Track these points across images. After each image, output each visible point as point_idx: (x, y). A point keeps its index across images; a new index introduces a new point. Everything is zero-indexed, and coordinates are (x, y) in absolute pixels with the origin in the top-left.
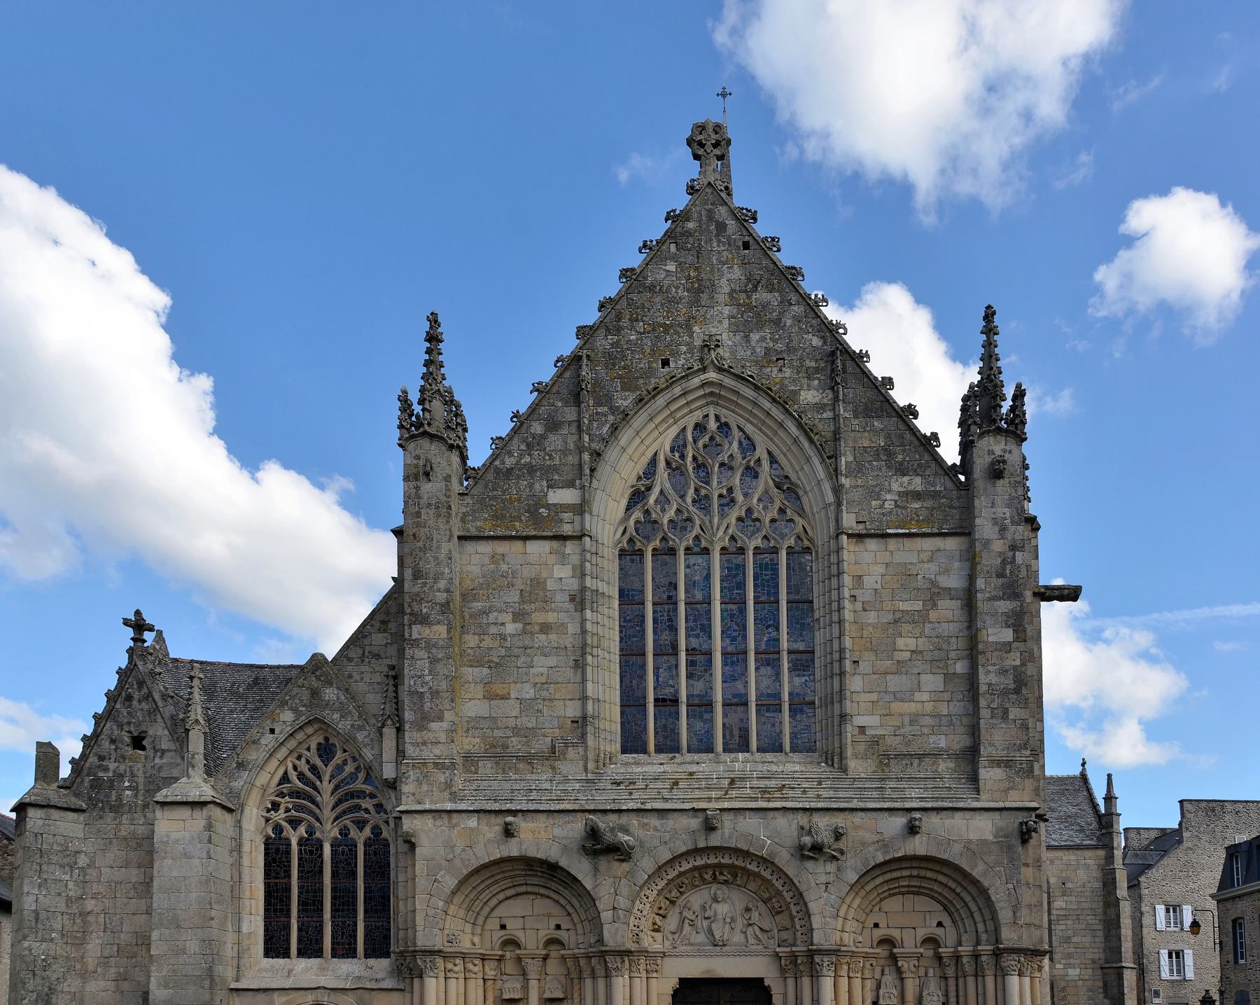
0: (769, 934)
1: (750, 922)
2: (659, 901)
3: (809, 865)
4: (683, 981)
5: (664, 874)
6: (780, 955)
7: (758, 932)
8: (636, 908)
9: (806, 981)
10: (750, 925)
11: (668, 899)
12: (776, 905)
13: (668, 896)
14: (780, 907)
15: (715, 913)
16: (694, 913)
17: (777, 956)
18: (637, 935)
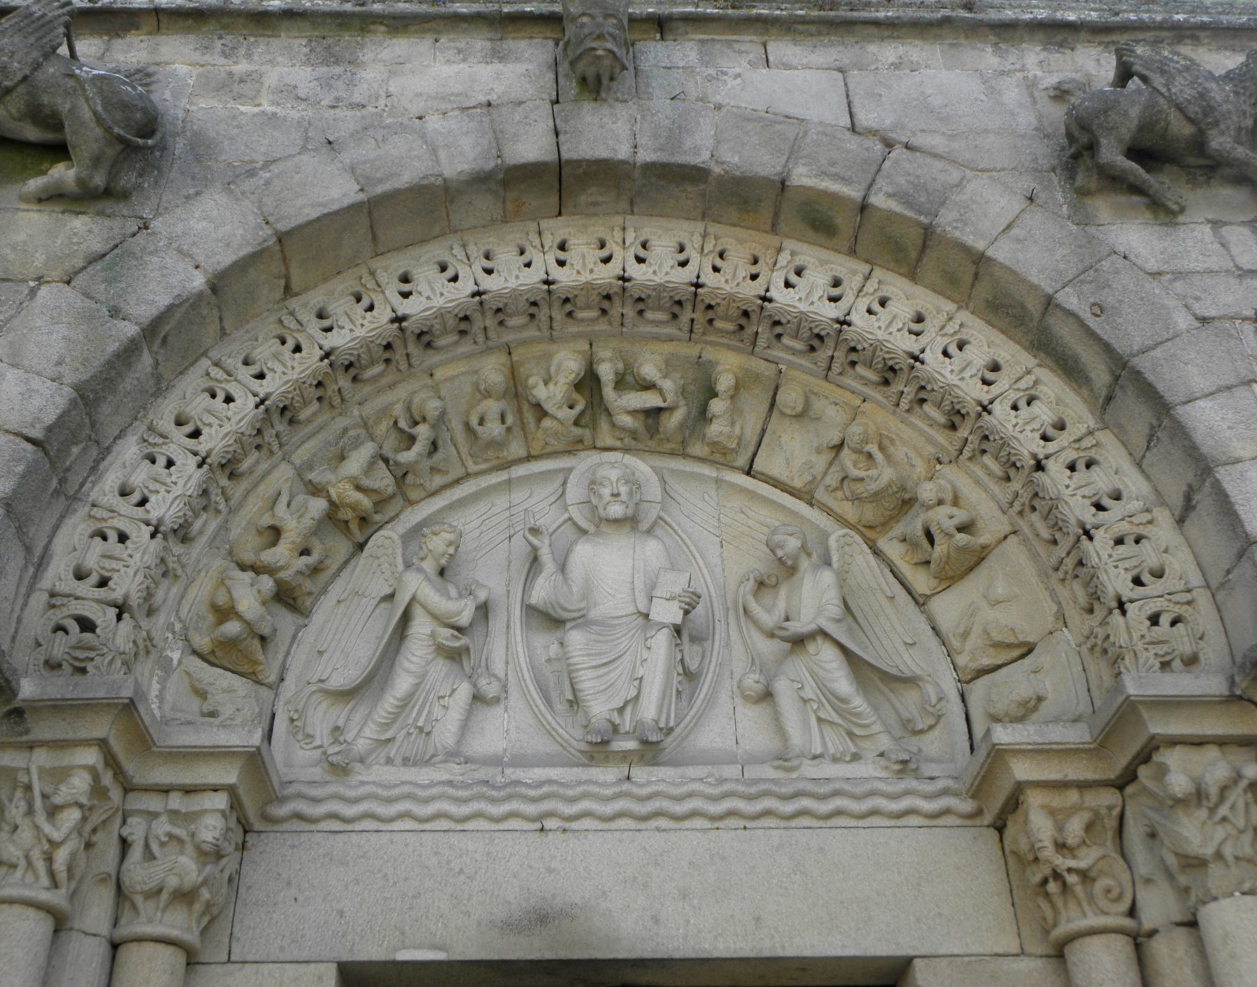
2: (266, 489)
5: (314, 326)
6: (1022, 770)
7: (843, 683)
8: (111, 479)
12: (943, 518)
15: (586, 594)
18: (87, 625)
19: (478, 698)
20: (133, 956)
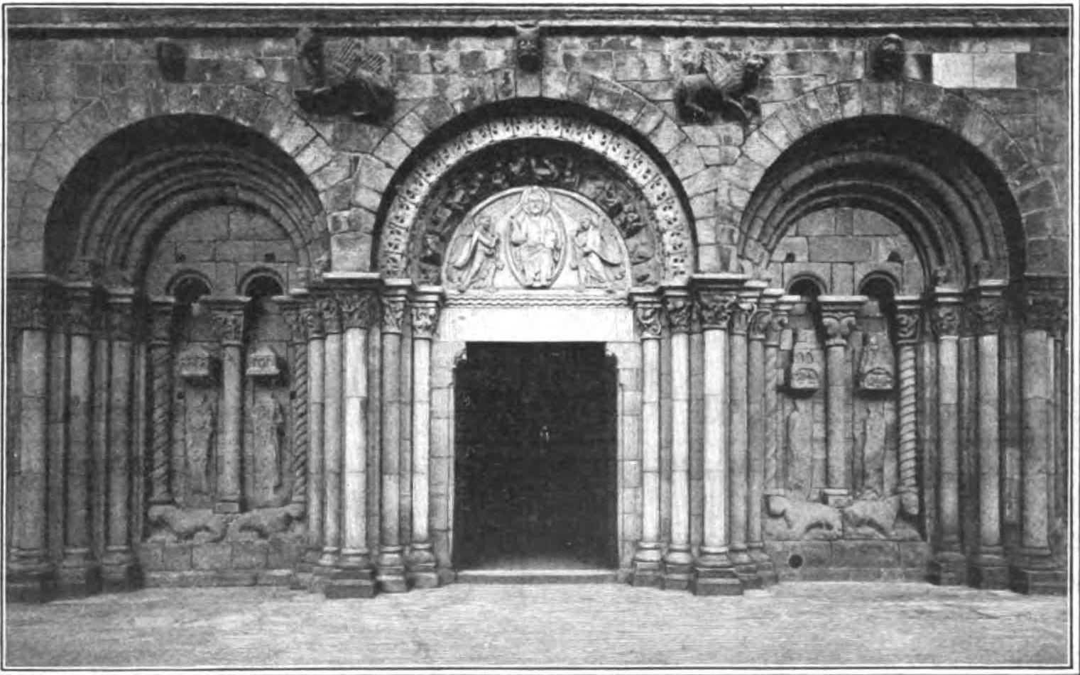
0: (616, 270)
1: (586, 250)
3: (697, 132)
4: (472, 347)
6: (637, 299)
9: (679, 343)
10: (587, 254)
11: (448, 206)
13: (450, 201)
14: (638, 220)
16: (493, 236)
17: (630, 302)
19: (497, 268)
20: (417, 343)
